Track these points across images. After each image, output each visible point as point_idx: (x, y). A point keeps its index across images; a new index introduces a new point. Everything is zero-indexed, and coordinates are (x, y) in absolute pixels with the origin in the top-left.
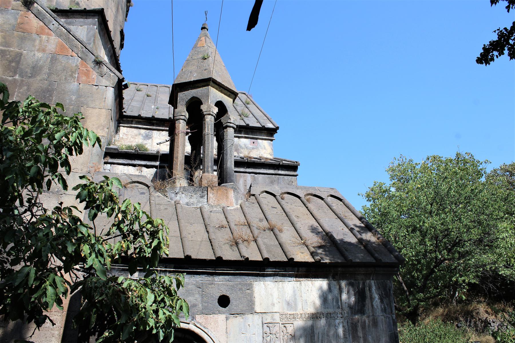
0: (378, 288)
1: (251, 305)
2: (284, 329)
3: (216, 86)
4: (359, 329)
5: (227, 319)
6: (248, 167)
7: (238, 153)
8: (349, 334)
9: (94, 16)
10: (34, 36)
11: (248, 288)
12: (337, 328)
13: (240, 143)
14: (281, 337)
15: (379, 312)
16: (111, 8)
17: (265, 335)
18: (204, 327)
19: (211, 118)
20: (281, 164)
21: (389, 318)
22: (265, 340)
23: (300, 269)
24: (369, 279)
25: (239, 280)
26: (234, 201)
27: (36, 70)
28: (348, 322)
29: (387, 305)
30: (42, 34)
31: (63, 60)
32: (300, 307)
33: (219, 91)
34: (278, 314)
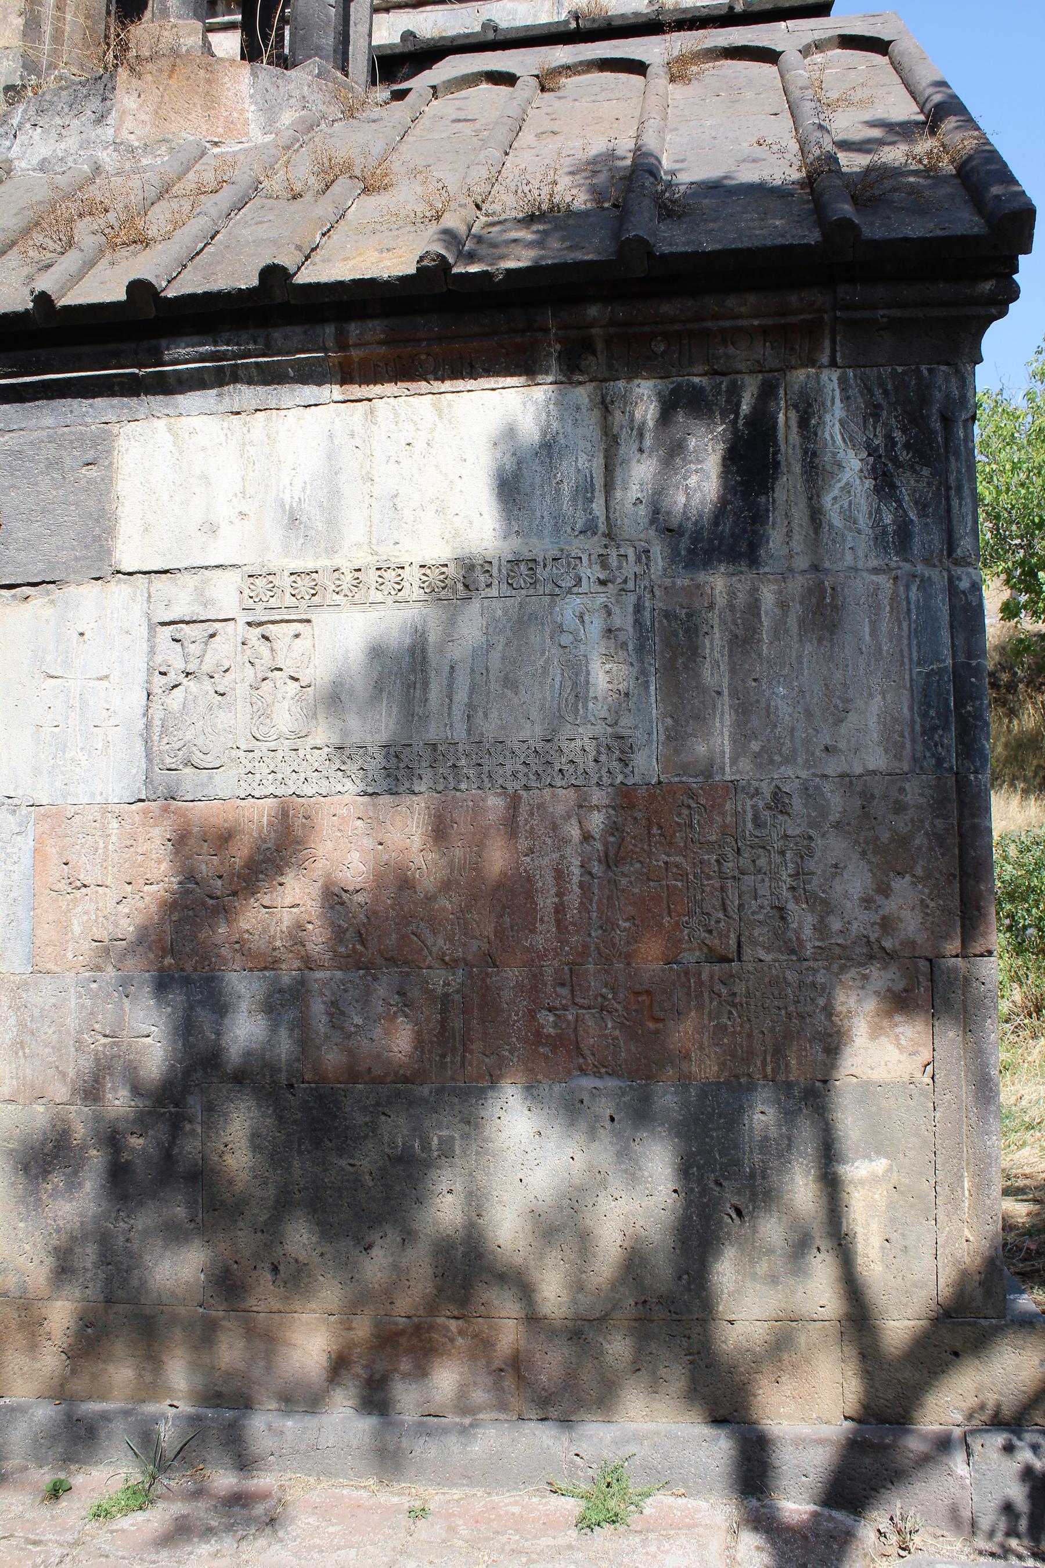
1: (97, 538)
2: (263, 648)
4: (715, 644)
8: (643, 672)
11: (90, 455)
12: (565, 639)
14: (242, 691)
17: (159, 681)
21: (925, 583)
22: (155, 705)
23: (354, 329)
24: (812, 363)
25: (49, 421)
26: (251, 111)
28: (638, 609)
29: (922, 507)
34: (232, 579)
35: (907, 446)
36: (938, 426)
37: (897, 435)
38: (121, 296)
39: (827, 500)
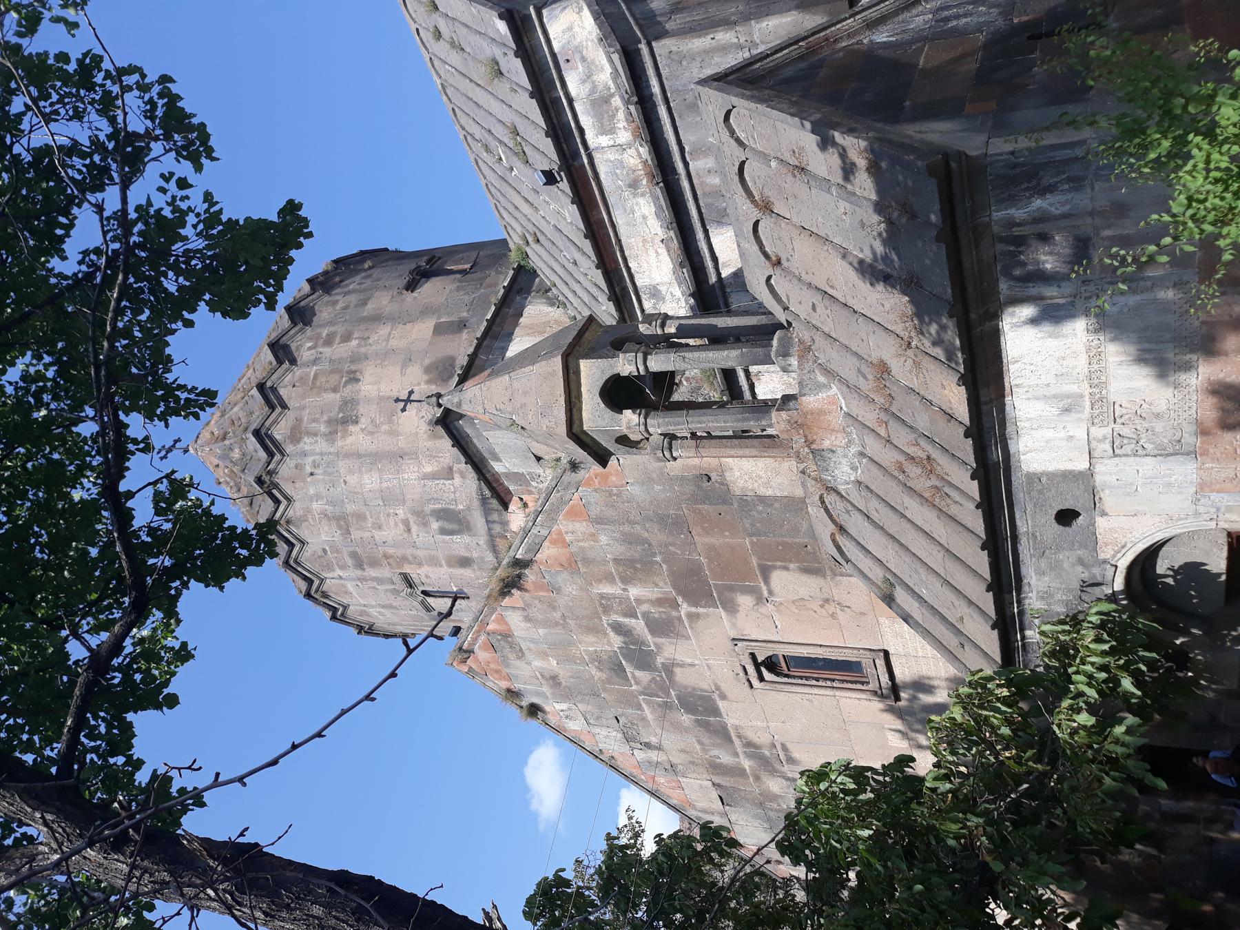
0: (1012, 200)
3: (575, 412)
5: (1104, 514)
6: (674, 170)
7: (612, 96)
9: (456, 428)
10: (574, 549)
13: (583, 94)
15: (1082, 200)
16: (387, 340)
18: (1123, 547)
19: (653, 426)
20: (635, 99)
23: (983, 399)
24: (989, 225)
27: (630, 540)
30: (564, 541)
31: (594, 511)
32: (1073, 388)
33: (581, 402)
35: (1029, 182)
36: (1018, 170)
37: (1023, 187)
38: (976, 482)
39: (1058, 212)
